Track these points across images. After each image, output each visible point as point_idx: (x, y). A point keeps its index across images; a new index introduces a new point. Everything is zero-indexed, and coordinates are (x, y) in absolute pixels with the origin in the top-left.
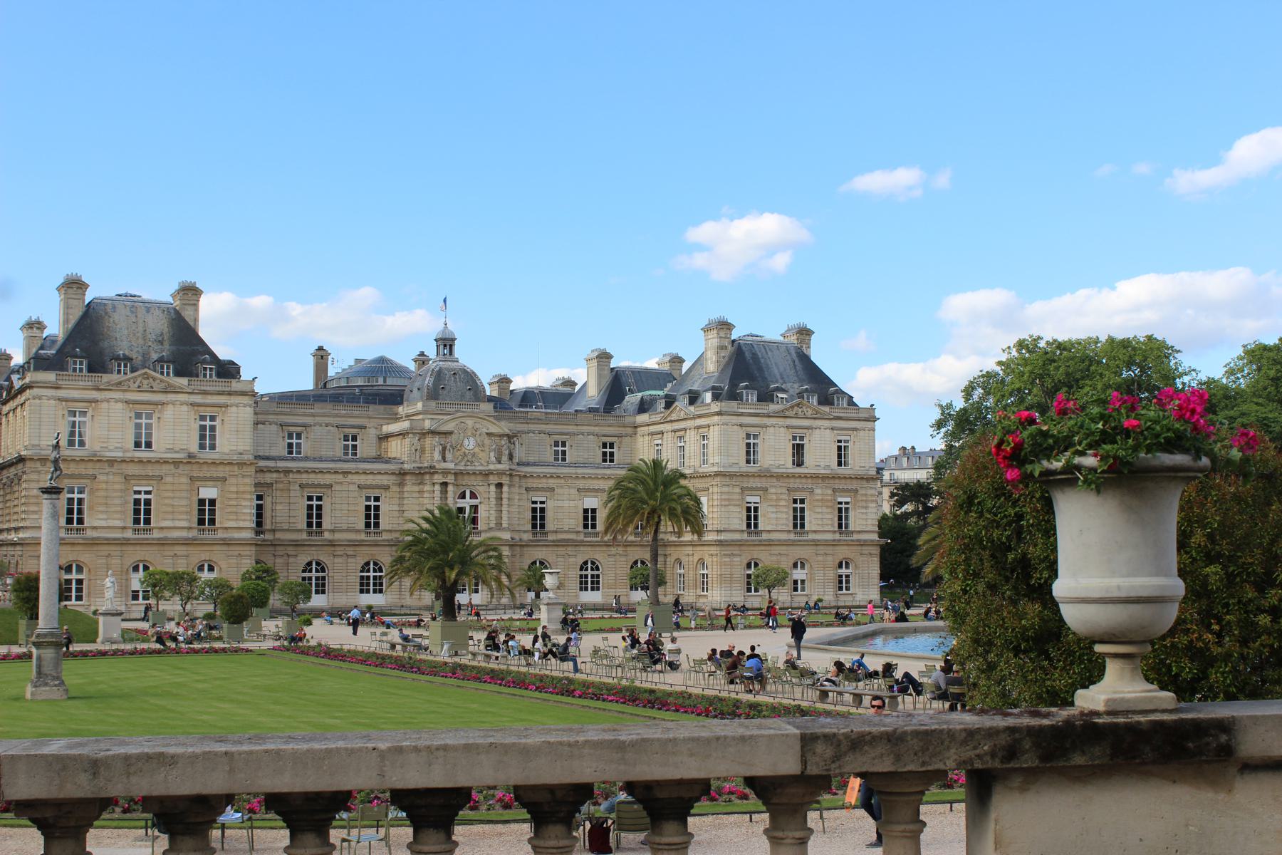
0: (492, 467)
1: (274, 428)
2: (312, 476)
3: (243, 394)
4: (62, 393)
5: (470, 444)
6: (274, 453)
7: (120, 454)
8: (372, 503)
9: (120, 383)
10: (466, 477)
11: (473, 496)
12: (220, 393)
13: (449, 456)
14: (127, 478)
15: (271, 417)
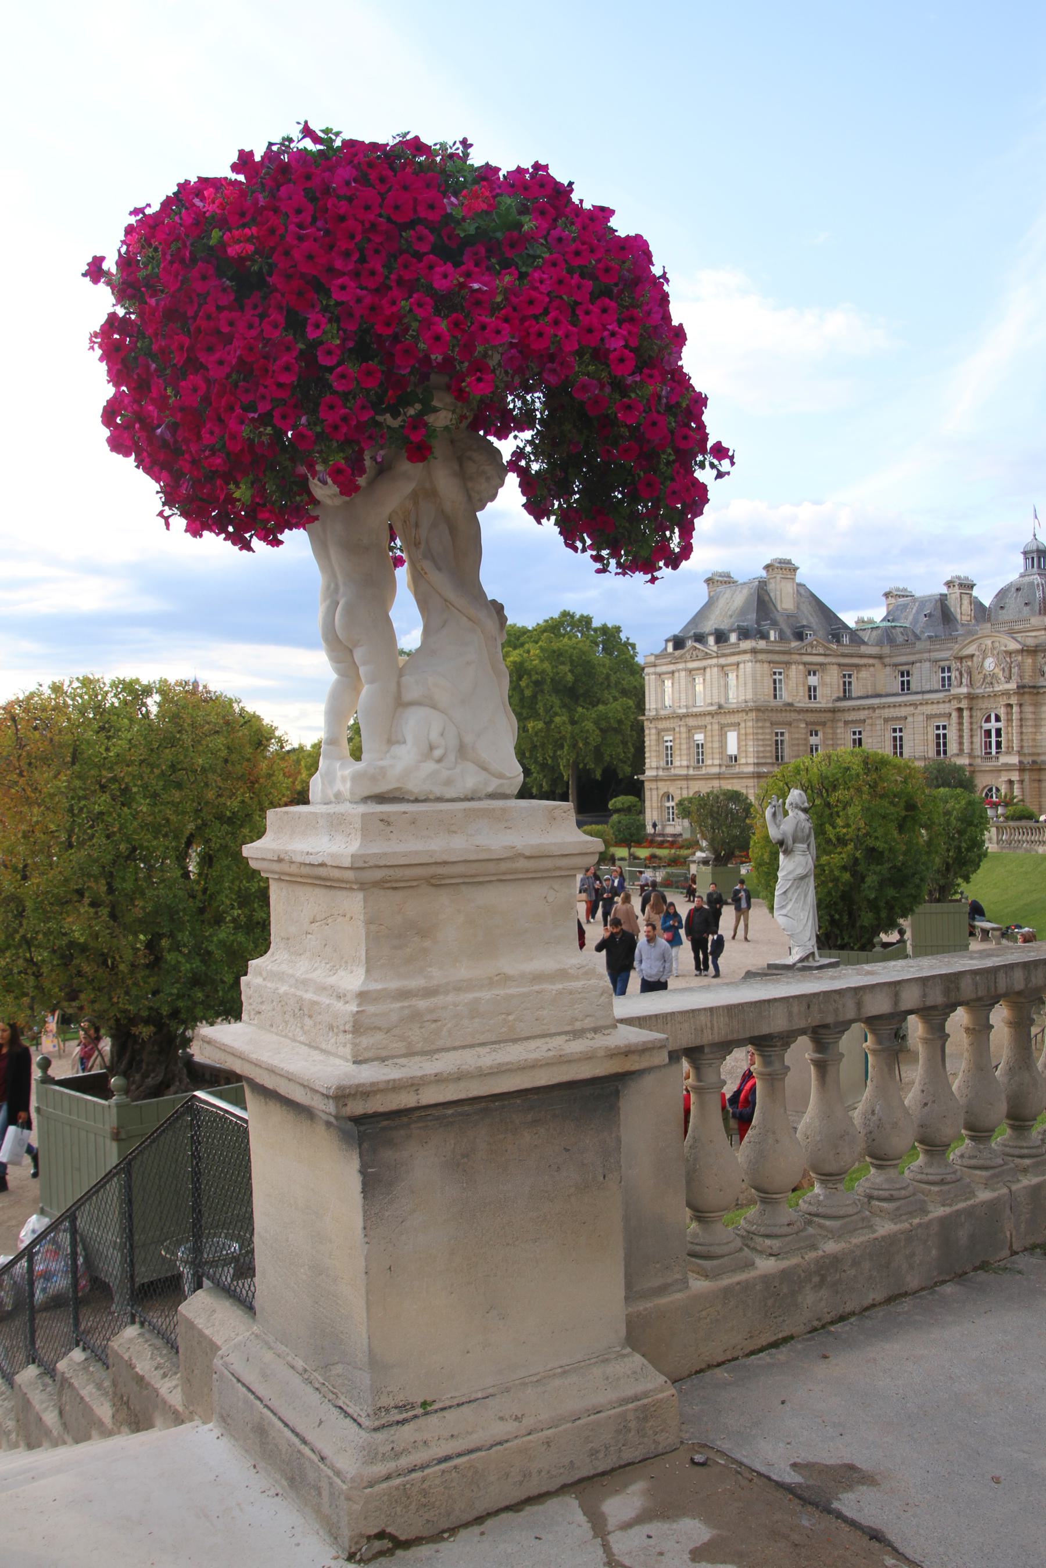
0: (1001, 688)
1: (927, 665)
2: (892, 710)
3: (745, 652)
4: (659, 669)
5: (990, 664)
6: (927, 688)
7: (684, 711)
8: (941, 732)
9: (681, 657)
10: (986, 700)
11: (998, 719)
12: (733, 654)
13: (964, 680)
14: (690, 730)
15: (926, 656)
